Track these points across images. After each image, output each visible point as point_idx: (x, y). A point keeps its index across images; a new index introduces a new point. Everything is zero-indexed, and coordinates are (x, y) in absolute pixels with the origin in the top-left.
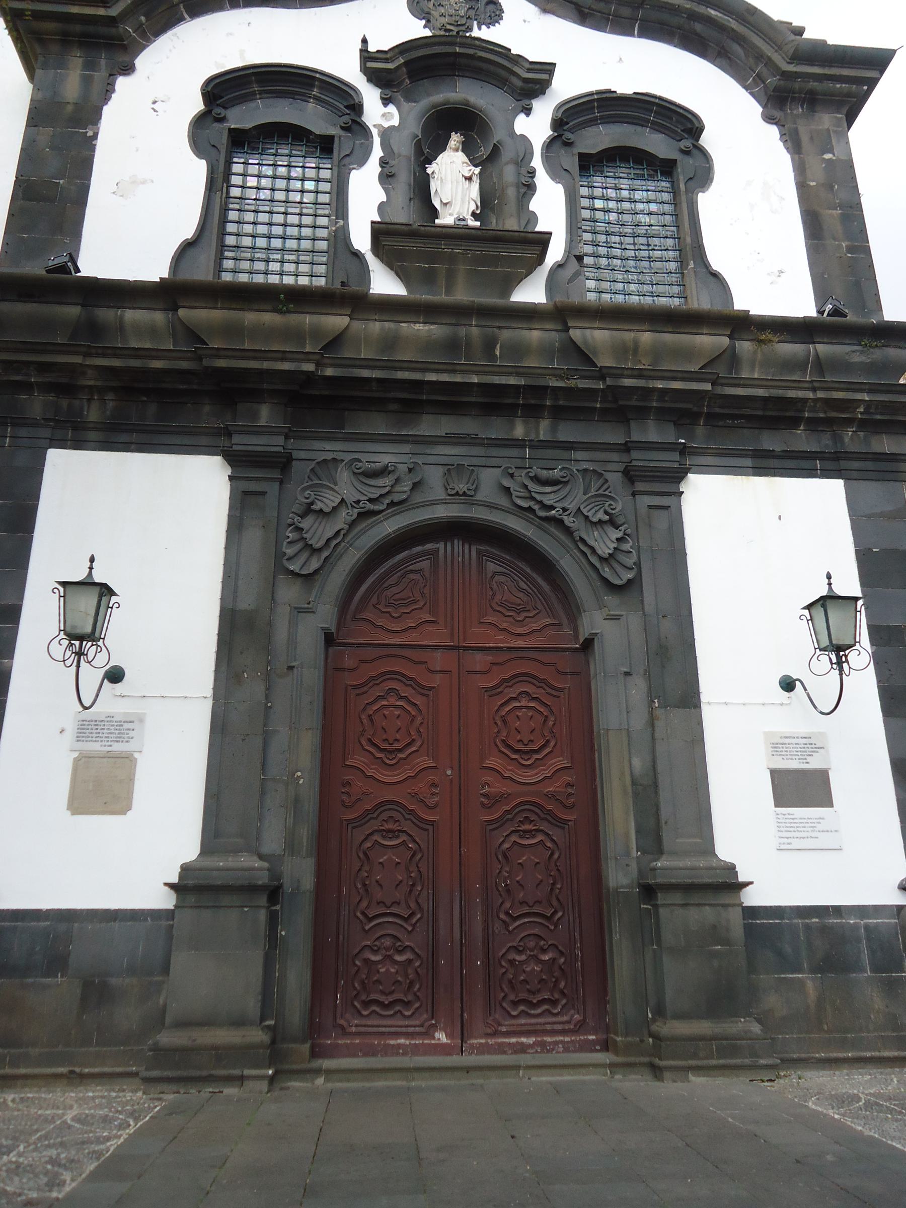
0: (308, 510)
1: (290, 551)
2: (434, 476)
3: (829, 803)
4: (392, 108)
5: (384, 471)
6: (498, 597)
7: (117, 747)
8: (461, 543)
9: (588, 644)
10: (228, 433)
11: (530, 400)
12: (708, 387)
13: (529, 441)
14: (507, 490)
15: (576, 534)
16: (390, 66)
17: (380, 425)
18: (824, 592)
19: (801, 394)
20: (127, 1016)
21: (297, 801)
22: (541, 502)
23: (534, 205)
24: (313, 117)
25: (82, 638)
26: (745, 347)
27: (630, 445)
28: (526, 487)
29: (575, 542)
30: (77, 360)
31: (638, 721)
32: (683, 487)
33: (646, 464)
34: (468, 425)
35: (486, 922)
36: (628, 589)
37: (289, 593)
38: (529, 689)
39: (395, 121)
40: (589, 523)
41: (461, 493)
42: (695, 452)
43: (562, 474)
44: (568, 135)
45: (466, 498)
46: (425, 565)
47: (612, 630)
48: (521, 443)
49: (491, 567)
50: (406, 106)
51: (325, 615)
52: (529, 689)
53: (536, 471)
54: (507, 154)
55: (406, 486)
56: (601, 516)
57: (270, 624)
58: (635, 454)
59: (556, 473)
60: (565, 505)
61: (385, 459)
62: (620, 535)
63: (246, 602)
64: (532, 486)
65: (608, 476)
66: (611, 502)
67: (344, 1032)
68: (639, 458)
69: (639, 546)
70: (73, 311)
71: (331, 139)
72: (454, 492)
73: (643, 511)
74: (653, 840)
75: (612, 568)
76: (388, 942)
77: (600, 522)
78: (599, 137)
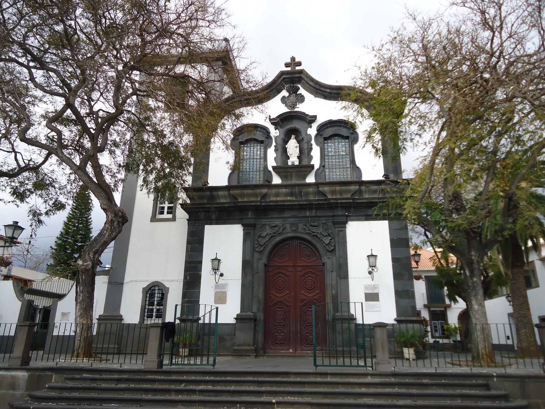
0: (260, 236)
1: (256, 246)
2: (288, 226)
3: (378, 301)
4: (277, 130)
7: (223, 290)
9: (324, 264)
11: (310, 206)
12: (352, 201)
16: (276, 121)
18: (370, 254)
19: (376, 200)
20: (228, 344)
24: (259, 136)
25: (215, 269)
26: (363, 188)
30: (210, 206)
31: (334, 283)
34: (295, 213)
35: (300, 327)
36: (333, 251)
37: (257, 255)
39: (278, 134)
44: (321, 133)
45: (295, 231)
46: (287, 246)
47: (329, 261)
49: (303, 246)
50: (281, 129)
51: (264, 260)
54: (305, 140)
55: (281, 229)
58: (335, 218)
61: (277, 223)
63: (248, 258)
64: (310, 228)
67: (271, 349)
68: (337, 219)
70: (208, 193)
71: (263, 141)
74: (336, 309)
76: (280, 331)
78: (329, 132)
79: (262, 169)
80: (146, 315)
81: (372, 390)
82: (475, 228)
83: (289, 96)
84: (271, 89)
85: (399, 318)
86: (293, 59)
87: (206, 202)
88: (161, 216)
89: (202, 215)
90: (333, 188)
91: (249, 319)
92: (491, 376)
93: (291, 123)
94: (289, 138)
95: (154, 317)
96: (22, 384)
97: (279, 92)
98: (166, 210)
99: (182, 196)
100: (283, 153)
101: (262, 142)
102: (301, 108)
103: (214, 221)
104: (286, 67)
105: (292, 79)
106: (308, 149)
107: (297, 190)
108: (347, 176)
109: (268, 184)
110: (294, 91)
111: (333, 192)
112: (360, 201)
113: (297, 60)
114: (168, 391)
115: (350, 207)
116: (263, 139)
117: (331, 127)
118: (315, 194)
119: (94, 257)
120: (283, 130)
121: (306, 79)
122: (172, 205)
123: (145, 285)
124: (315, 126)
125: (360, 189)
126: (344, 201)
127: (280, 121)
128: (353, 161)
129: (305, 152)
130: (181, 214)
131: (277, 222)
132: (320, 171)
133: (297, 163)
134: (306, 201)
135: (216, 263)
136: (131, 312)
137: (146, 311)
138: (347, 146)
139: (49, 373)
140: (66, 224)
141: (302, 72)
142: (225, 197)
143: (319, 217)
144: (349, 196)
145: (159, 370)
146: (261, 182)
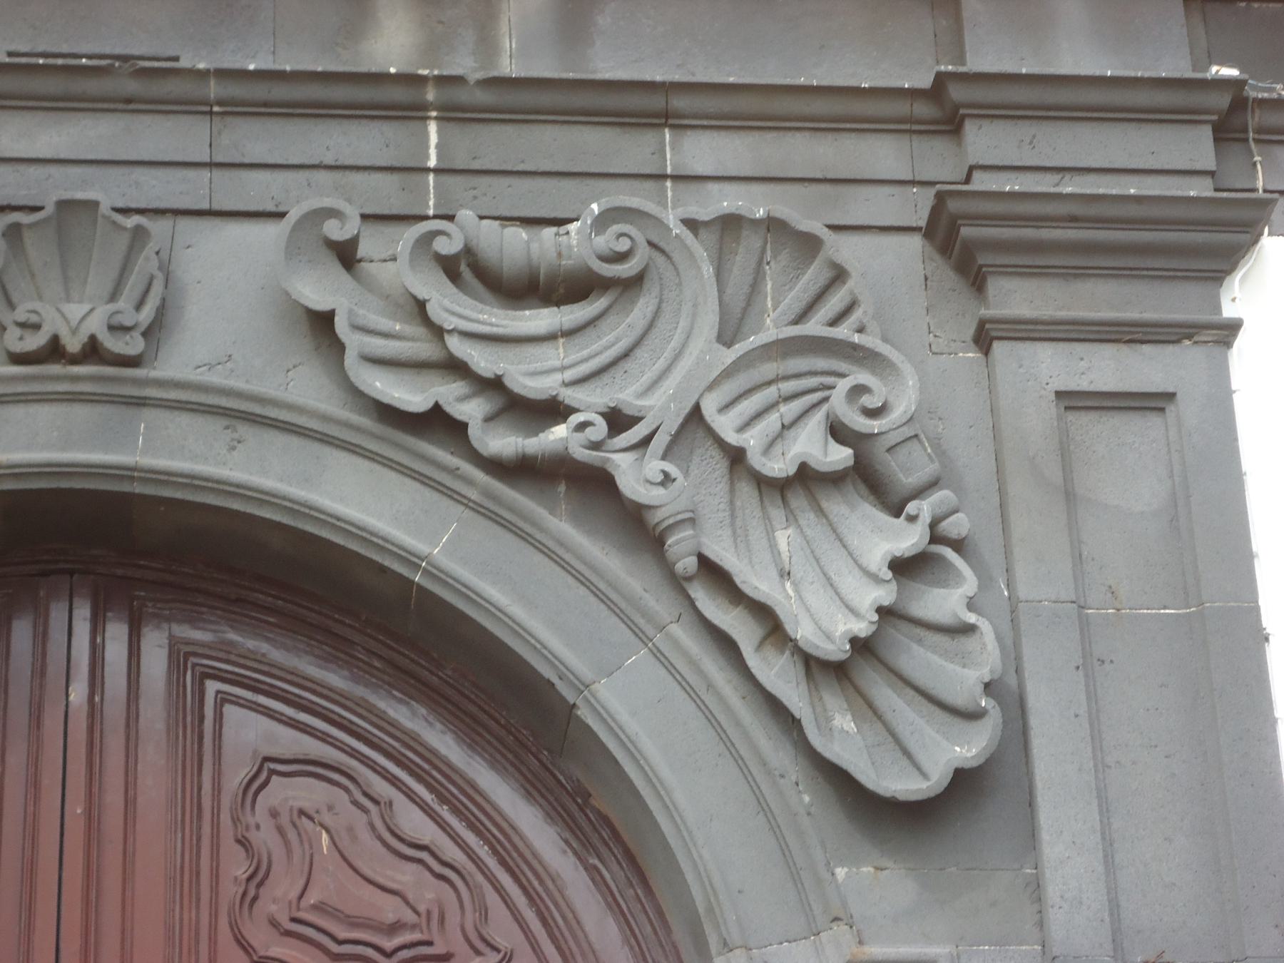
6: (280, 894)
8: (83, 612)
13: (442, 81)
14: (322, 322)
15: (680, 547)
22: (494, 385)
27: (957, 93)
28: (421, 306)
29: (678, 583)
32: (1240, 297)
33: (1043, 184)
40: (746, 491)
41: (73, 345)
43: (604, 242)
48: (398, 94)
49: (248, 732)
53: (471, 228)
56: (813, 446)
58: (985, 141)
59: (576, 244)
60: (624, 393)
62: (907, 539)
64: (454, 307)
65: (846, 249)
66: (863, 377)
69: (1013, 602)
72: (34, 342)
73: (1034, 417)
75: (869, 710)
77: (806, 477)
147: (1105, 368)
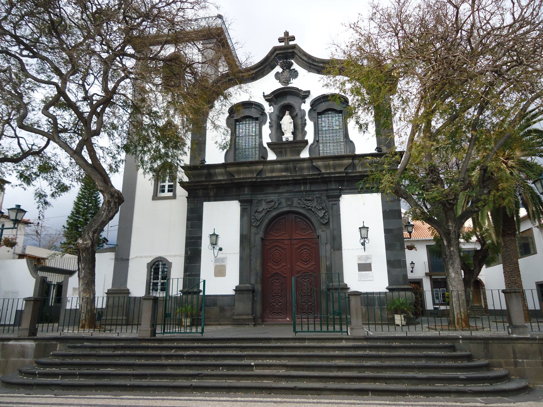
0: (256, 212)
2: (283, 201)
4: (272, 107)
5: (272, 201)
7: (222, 264)
9: (318, 237)
10: (239, 195)
11: (304, 181)
12: (345, 175)
16: (270, 98)
17: (271, 190)
20: (228, 314)
21: (257, 273)
23: (306, 129)
24: (253, 112)
25: (214, 244)
26: (356, 161)
31: (328, 254)
32: (340, 199)
36: (327, 224)
37: (253, 230)
38: (306, 247)
42: (344, 189)
44: (315, 108)
45: (290, 206)
47: (323, 234)
49: (298, 220)
50: (275, 106)
51: (261, 234)
52: (306, 247)
54: (299, 116)
55: (277, 204)
57: (250, 237)
58: (329, 192)
61: (273, 198)
63: (245, 233)
64: (305, 202)
68: (331, 193)
70: (205, 171)
74: (330, 278)
78: (323, 106)
79: (257, 145)
80: (151, 288)
81: (344, 353)
82: (450, 200)
83: (283, 71)
84: (264, 65)
85: (391, 287)
86: (286, 33)
87: (204, 179)
88: (163, 195)
89: (200, 193)
90: (327, 163)
91: (248, 290)
92: (457, 339)
93: (285, 99)
94: (284, 115)
95: (159, 290)
96: (31, 352)
97: (273, 68)
98: (166, 189)
99: (182, 176)
100: (278, 129)
101: (257, 119)
102: (295, 83)
103: (212, 198)
104: (280, 42)
105: (286, 54)
106: (302, 124)
107: (291, 165)
108: (341, 151)
109: (263, 160)
110: (287, 66)
111: (327, 167)
112: (353, 175)
113: (290, 35)
114: (159, 357)
115: (344, 181)
116: (258, 116)
117: (324, 101)
118: (309, 168)
119: (93, 236)
120: (277, 106)
121: (299, 54)
122: (172, 183)
123: (149, 260)
124: (308, 101)
125: (353, 162)
126: (337, 175)
127: (274, 98)
128: (346, 135)
129: (299, 128)
130: (181, 192)
131: (273, 197)
132: (314, 146)
133: (291, 139)
134: (300, 176)
135: (214, 238)
136: (137, 285)
137: (152, 284)
138: (341, 120)
139: (54, 343)
140: (76, 204)
141: (295, 47)
142: (221, 174)
143: (314, 191)
144: (342, 170)
145: (152, 338)
146: (257, 159)
147: (334, 203)
